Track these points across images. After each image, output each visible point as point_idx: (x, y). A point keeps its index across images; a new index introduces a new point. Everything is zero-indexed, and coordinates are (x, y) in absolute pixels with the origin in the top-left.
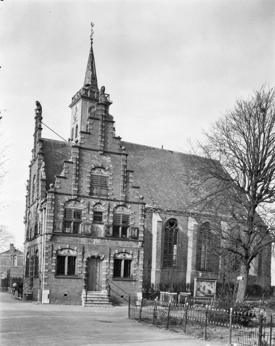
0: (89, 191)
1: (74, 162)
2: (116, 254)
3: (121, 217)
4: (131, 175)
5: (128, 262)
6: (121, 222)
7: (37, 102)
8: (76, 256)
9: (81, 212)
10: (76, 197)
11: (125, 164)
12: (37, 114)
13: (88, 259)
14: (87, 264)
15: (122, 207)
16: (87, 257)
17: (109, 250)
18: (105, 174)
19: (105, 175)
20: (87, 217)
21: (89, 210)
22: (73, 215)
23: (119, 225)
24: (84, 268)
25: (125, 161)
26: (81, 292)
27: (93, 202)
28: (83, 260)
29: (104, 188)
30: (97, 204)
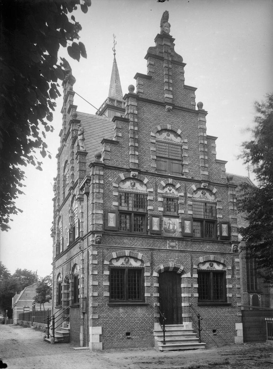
10: (137, 173)
20: (154, 207)
21: (156, 195)
28: (152, 274)
29: (176, 162)
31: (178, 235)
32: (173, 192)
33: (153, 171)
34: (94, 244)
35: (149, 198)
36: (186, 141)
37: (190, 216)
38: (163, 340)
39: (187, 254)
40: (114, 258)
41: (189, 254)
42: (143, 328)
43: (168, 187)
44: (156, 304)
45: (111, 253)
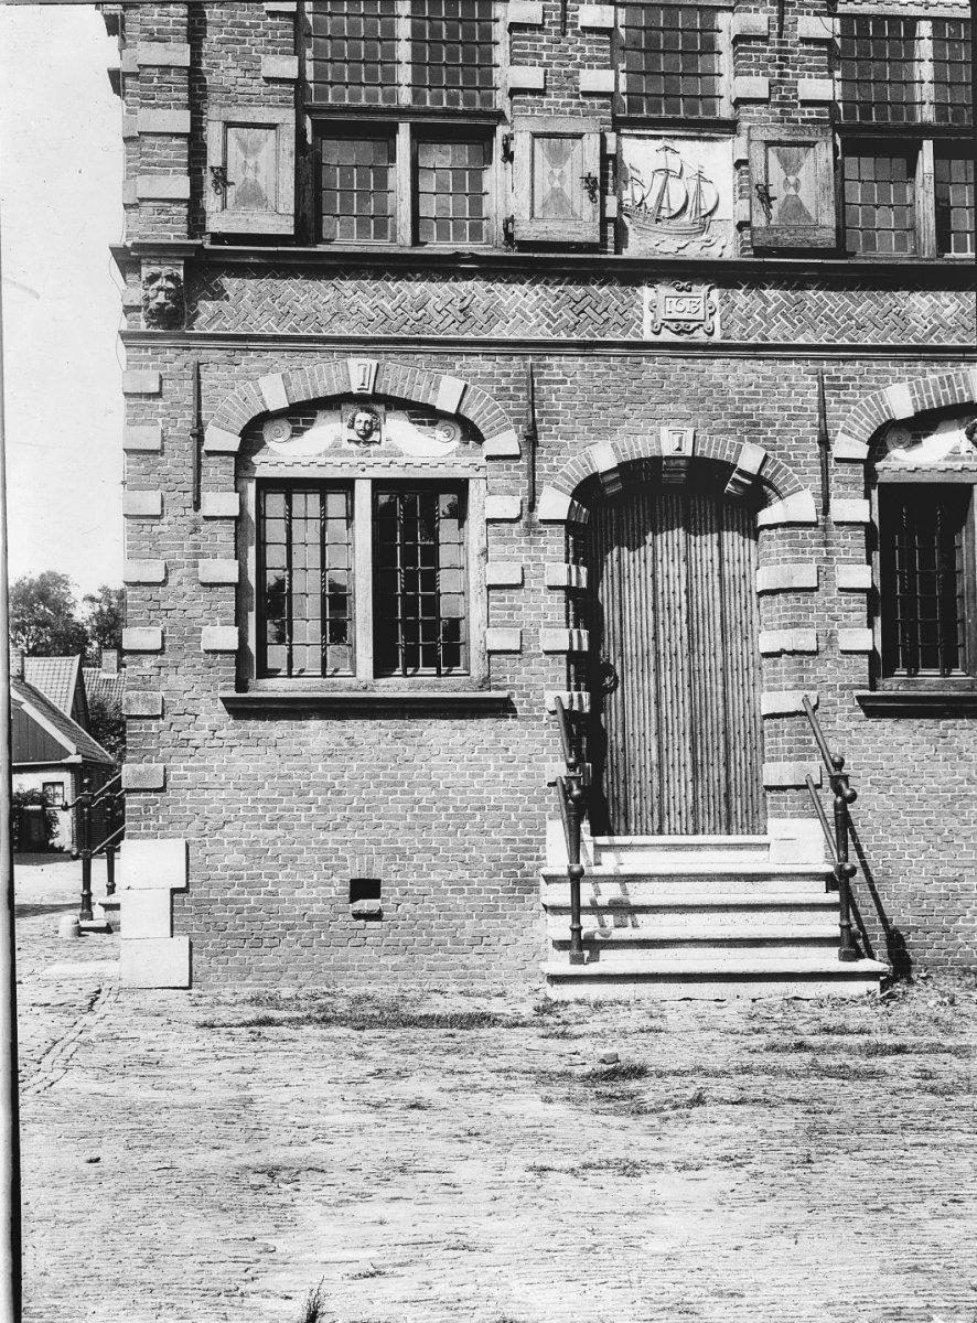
2: (891, 439)
3: (925, 48)
13: (588, 490)
31: (724, 245)
34: (143, 327)
37: (812, 113)
38: (567, 935)
39: (793, 365)
40: (272, 409)
41: (801, 366)
42: (466, 850)
45: (254, 379)
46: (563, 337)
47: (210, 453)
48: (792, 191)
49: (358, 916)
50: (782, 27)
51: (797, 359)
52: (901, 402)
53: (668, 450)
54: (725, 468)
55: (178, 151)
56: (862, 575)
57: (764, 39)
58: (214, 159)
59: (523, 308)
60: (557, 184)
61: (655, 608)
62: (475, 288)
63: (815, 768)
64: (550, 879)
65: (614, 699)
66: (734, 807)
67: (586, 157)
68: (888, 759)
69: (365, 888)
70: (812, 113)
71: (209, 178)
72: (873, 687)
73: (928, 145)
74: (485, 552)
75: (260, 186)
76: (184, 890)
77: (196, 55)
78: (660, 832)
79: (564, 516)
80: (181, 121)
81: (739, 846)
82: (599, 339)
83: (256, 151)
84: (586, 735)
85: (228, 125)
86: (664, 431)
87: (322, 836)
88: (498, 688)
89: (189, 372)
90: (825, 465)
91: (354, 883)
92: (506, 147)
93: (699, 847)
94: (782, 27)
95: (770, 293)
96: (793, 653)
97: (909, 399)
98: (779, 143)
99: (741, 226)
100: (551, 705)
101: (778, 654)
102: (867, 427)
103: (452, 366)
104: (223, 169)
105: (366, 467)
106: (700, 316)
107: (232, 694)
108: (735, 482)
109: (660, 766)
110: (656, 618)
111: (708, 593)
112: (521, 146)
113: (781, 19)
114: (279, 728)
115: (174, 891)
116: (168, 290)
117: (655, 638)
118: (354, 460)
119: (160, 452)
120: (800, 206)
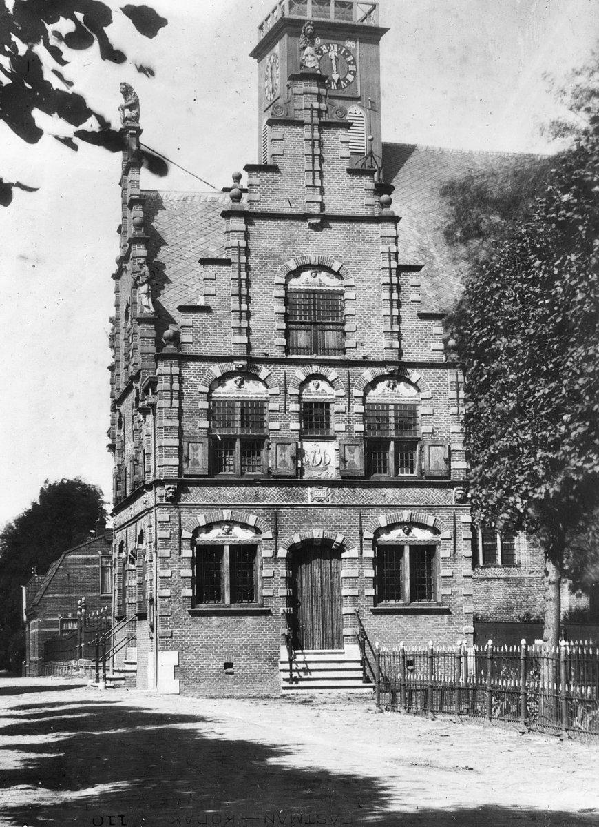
0: (283, 341)
1: (234, 258)
2: (381, 531)
3: (392, 413)
4: (411, 279)
5: (424, 554)
6: (392, 427)
7: (125, 84)
8: (255, 543)
9: (263, 408)
10: (245, 363)
11: (394, 249)
12: (125, 119)
14: (288, 568)
15: (392, 381)
16: (289, 544)
17: (358, 520)
18: (327, 282)
19: (332, 289)
20: (283, 422)
22: (238, 417)
23: (386, 438)
24: (282, 578)
25: (393, 240)
26: (277, 654)
27: (300, 373)
28: (276, 553)
30: (310, 378)
31: (332, 474)
32: (323, 390)
33: (279, 354)
34: (164, 502)
35: (271, 406)
36: (351, 282)
37: (358, 434)
38: (289, 677)
39: (352, 511)
43: (312, 382)
44: (284, 610)
46: (285, 503)
47: (183, 539)
48: (352, 459)
49: (227, 673)
50: (349, 409)
51: (353, 509)
52: (383, 522)
53: (316, 536)
54: (332, 541)
55: (175, 451)
56: (371, 573)
57: (344, 413)
58: (185, 453)
59: (273, 494)
60: (283, 458)
61: (311, 583)
62: (260, 490)
63: (357, 629)
64: (282, 662)
65: (299, 610)
66: (334, 641)
67: (290, 450)
68: (379, 627)
69: (228, 665)
70: (358, 434)
71: (184, 459)
72: (375, 606)
73: (392, 443)
74: (262, 567)
75: (199, 456)
76: (178, 666)
77: (180, 422)
78: (313, 649)
79: (285, 556)
80: (176, 442)
81: (336, 653)
82: (295, 503)
83: (197, 450)
84: (293, 620)
85: (189, 442)
86: (314, 531)
87: (216, 650)
88: (267, 607)
89: (177, 514)
90: (361, 542)
91: (225, 664)
92: (268, 446)
93: (324, 653)
94: (349, 409)
95: (345, 489)
96: (352, 596)
97: (385, 521)
98: (348, 445)
99: (337, 469)
100: (281, 612)
101: (347, 596)
102: (374, 528)
103: (252, 512)
104: (188, 456)
105: (230, 540)
106: (325, 496)
107: (190, 609)
108: (335, 545)
109: (313, 630)
110: (312, 585)
111: (327, 578)
112: (273, 446)
113: (349, 407)
114: (204, 619)
115: (175, 666)
116: (173, 492)
117: (312, 591)
118: (224, 539)
119: (170, 538)
120: (354, 463)
